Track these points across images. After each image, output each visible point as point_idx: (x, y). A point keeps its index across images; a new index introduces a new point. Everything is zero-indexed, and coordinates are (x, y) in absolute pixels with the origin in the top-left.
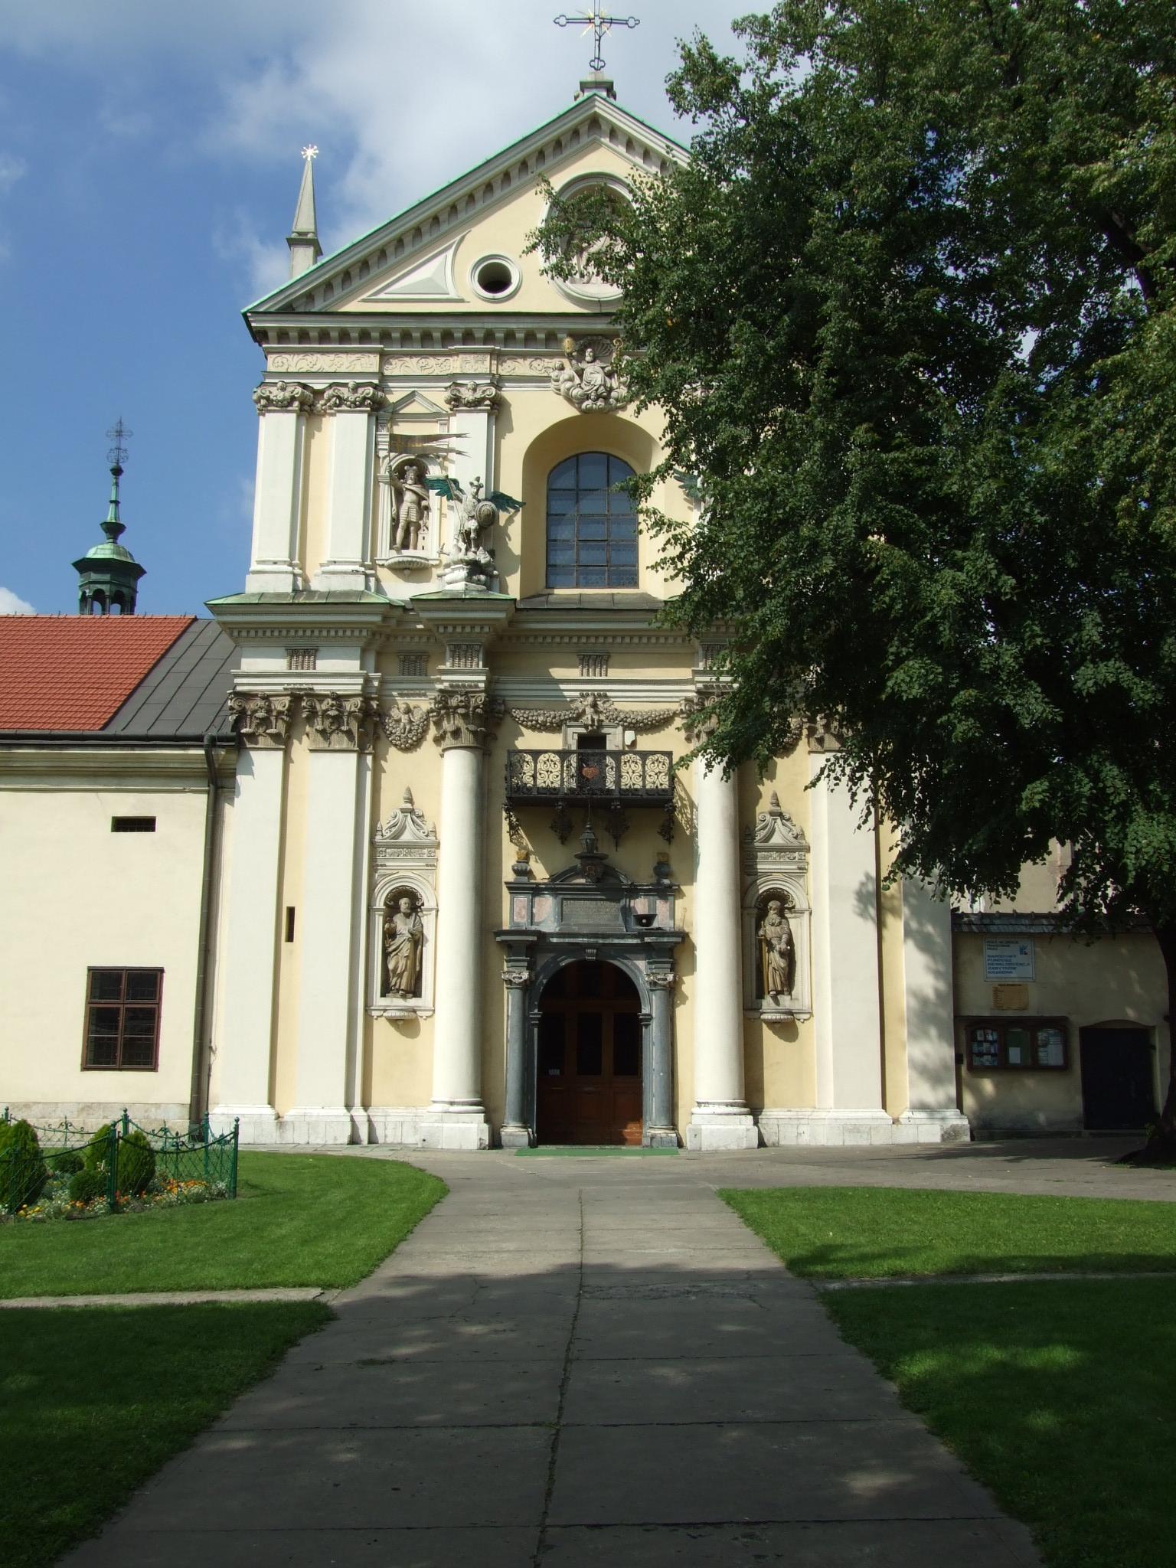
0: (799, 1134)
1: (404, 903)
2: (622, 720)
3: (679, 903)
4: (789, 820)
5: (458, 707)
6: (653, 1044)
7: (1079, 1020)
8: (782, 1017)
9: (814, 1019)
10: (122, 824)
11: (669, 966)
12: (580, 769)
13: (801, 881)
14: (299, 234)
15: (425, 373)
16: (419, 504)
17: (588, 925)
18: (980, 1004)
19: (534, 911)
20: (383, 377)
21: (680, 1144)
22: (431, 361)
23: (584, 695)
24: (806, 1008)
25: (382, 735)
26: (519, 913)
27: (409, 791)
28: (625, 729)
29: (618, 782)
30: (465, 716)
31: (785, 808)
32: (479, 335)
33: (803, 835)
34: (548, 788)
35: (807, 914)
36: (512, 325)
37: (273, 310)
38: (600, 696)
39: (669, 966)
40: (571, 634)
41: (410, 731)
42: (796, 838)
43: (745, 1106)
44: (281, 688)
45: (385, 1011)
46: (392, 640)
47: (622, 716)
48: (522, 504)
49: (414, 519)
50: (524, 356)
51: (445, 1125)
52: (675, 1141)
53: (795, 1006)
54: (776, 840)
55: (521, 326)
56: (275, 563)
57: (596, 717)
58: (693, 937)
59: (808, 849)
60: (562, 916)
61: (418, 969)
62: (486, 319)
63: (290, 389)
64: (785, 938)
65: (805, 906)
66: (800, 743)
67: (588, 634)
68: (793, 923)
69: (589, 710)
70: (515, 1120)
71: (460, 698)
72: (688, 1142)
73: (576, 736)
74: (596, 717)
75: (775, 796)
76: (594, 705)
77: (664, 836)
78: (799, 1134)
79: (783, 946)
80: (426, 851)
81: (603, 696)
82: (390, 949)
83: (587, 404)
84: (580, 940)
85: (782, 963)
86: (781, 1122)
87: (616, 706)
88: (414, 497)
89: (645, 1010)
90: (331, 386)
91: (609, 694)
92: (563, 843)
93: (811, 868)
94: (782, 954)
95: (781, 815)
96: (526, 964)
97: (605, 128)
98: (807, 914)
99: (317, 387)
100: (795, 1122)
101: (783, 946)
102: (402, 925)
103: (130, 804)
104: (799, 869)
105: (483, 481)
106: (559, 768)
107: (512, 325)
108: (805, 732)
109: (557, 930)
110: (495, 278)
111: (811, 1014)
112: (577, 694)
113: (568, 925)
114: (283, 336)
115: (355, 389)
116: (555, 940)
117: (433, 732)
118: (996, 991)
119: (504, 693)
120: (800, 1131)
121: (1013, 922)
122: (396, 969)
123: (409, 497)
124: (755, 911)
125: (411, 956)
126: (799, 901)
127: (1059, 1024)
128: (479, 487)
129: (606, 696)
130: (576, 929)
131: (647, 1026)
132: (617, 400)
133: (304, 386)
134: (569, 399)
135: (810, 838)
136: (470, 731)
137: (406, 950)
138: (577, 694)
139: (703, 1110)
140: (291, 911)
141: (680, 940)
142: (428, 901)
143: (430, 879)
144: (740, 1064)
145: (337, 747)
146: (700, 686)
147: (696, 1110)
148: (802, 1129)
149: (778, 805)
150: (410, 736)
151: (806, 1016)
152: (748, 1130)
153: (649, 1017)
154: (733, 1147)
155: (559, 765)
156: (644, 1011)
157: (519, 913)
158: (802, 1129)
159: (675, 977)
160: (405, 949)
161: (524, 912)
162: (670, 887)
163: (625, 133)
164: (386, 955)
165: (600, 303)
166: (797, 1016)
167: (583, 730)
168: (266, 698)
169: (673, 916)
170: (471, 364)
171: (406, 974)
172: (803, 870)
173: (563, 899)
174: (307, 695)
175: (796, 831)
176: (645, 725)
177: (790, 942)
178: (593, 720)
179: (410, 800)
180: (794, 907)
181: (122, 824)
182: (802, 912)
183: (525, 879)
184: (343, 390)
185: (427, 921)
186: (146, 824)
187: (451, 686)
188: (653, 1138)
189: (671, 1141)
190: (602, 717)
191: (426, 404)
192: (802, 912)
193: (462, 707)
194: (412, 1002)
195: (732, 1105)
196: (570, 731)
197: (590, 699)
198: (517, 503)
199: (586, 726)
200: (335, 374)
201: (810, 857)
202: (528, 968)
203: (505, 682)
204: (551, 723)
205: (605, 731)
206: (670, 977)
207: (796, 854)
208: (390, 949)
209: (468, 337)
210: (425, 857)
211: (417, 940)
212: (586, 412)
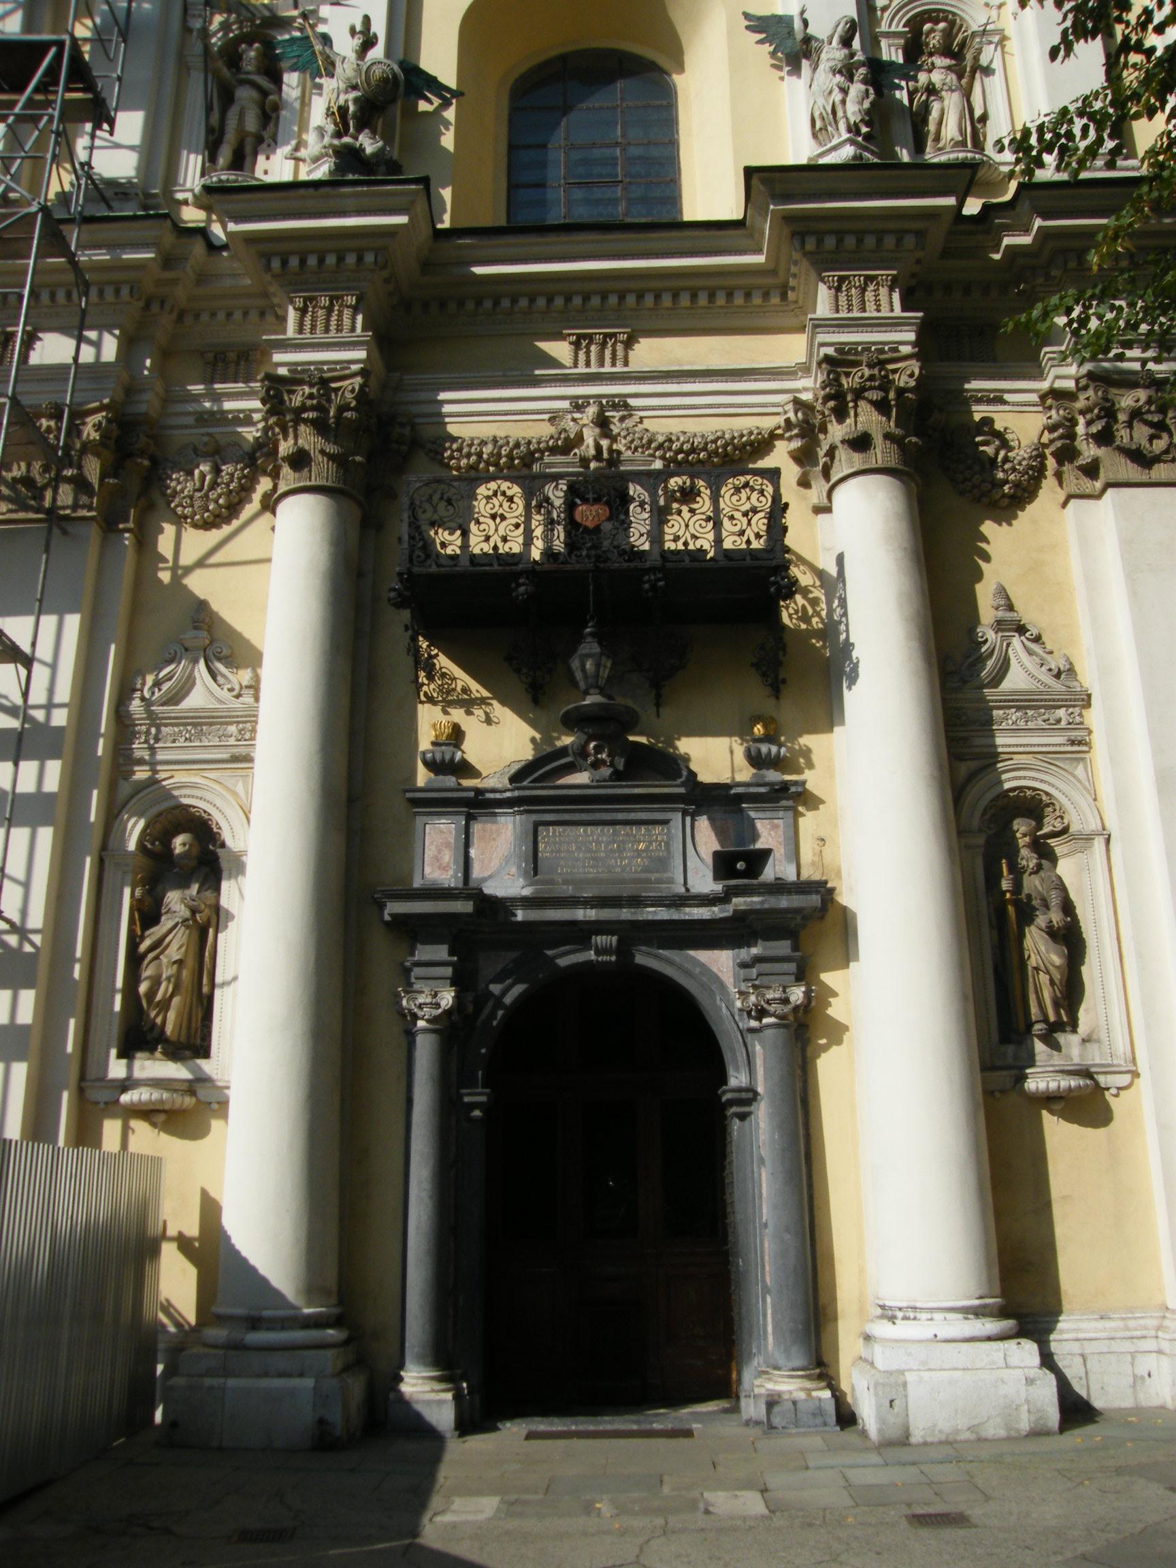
0: (1137, 1381)
2: (660, 446)
3: (809, 823)
4: (1037, 639)
5: (303, 408)
6: (762, 1161)
8: (1074, 1082)
9: (1143, 1083)
11: (792, 967)
12: (570, 507)
13: (1079, 771)
16: (262, 106)
17: (595, 881)
19: (473, 852)
21: (846, 1418)
23: (578, 405)
24: (1120, 1061)
25: (161, 503)
26: (437, 858)
29: (656, 536)
30: (320, 426)
31: (1027, 612)
33: (1071, 671)
34: (497, 556)
35: (1099, 843)
38: (615, 407)
39: (792, 967)
41: (214, 486)
42: (1058, 676)
43: (1002, 1313)
46: (189, 320)
47: (661, 439)
48: (457, 94)
51: (232, 1382)
52: (830, 1408)
53: (1095, 1057)
54: (1015, 680)
57: (605, 443)
58: (844, 898)
59: (1087, 701)
60: (534, 865)
61: (205, 989)
64: (1054, 899)
65: (1093, 825)
66: (1045, 483)
68: (1065, 868)
69: (590, 436)
70: (422, 1360)
71: (307, 390)
72: (867, 1411)
74: (605, 443)
75: (1002, 592)
76: (602, 423)
77: (764, 675)
78: (1137, 1380)
79: (1056, 917)
80: (233, 729)
81: (620, 403)
84: (580, 914)
85: (1056, 959)
86: (1090, 1348)
87: (647, 424)
88: (254, 94)
89: (737, 1079)
91: (631, 402)
92: (536, 701)
93: (1098, 740)
94: (1053, 933)
95: (1021, 629)
96: (448, 971)
98: (1099, 843)
100: (1127, 1346)
101: (1056, 917)
104: (1072, 743)
105: (379, 27)
106: (521, 510)
108: (1051, 463)
109: (527, 892)
111: (1135, 1074)
112: (565, 404)
113: (552, 882)
116: (520, 915)
119: (415, 409)
120: (1141, 1370)
123: (245, 95)
124: (980, 840)
125: (191, 963)
126: (1080, 817)
128: (368, 43)
129: (626, 406)
130: (569, 890)
131: (743, 1117)
135: (1088, 677)
136: (331, 457)
138: (565, 404)
139: (902, 1330)
141: (815, 900)
143: (240, 788)
144: (983, 1212)
146: (830, 351)
147: (882, 1329)
148: (1147, 1363)
149: (1010, 607)
150: (213, 495)
151: (1124, 1080)
152: (1030, 1381)
153: (749, 1097)
154: (994, 1430)
155: (519, 501)
156: (733, 1082)
157: (437, 858)
158: (1147, 1363)
159: (807, 994)
160: (174, 946)
161: (447, 856)
162: (784, 787)
164: (135, 960)
166: (1102, 1079)
169: (795, 855)
171: (176, 1001)
172: (1080, 743)
173: (537, 825)
175: (1056, 662)
177: (1068, 907)
178: (598, 448)
180: (1065, 831)
182: (1088, 838)
183: (450, 781)
188: (772, 1402)
189: (819, 1412)
190: (620, 446)
192: (1088, 838)
193: (313, 408)
195: (978, 1312)
197: (592, 411)
198: (448, 89)
199: (584, 461)
201: (1094, 717)
202: (455, 981)
203: (418, 403)
204: (511, 457)
206: (797, 994)
207: (1061, 713)
208: (143, 947)
210: (232, 741)
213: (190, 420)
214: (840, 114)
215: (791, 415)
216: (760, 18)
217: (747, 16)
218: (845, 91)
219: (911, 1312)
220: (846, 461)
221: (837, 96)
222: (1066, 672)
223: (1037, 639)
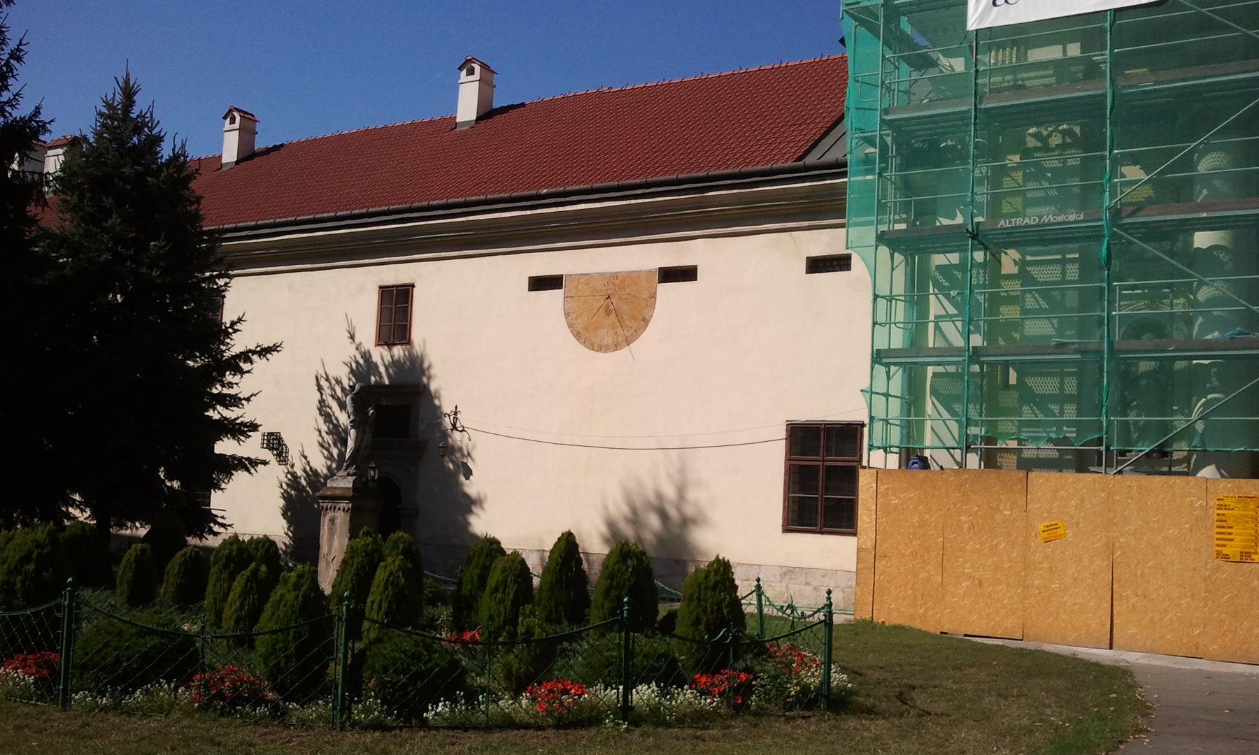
10: (817, 265)
181: (817, 265)
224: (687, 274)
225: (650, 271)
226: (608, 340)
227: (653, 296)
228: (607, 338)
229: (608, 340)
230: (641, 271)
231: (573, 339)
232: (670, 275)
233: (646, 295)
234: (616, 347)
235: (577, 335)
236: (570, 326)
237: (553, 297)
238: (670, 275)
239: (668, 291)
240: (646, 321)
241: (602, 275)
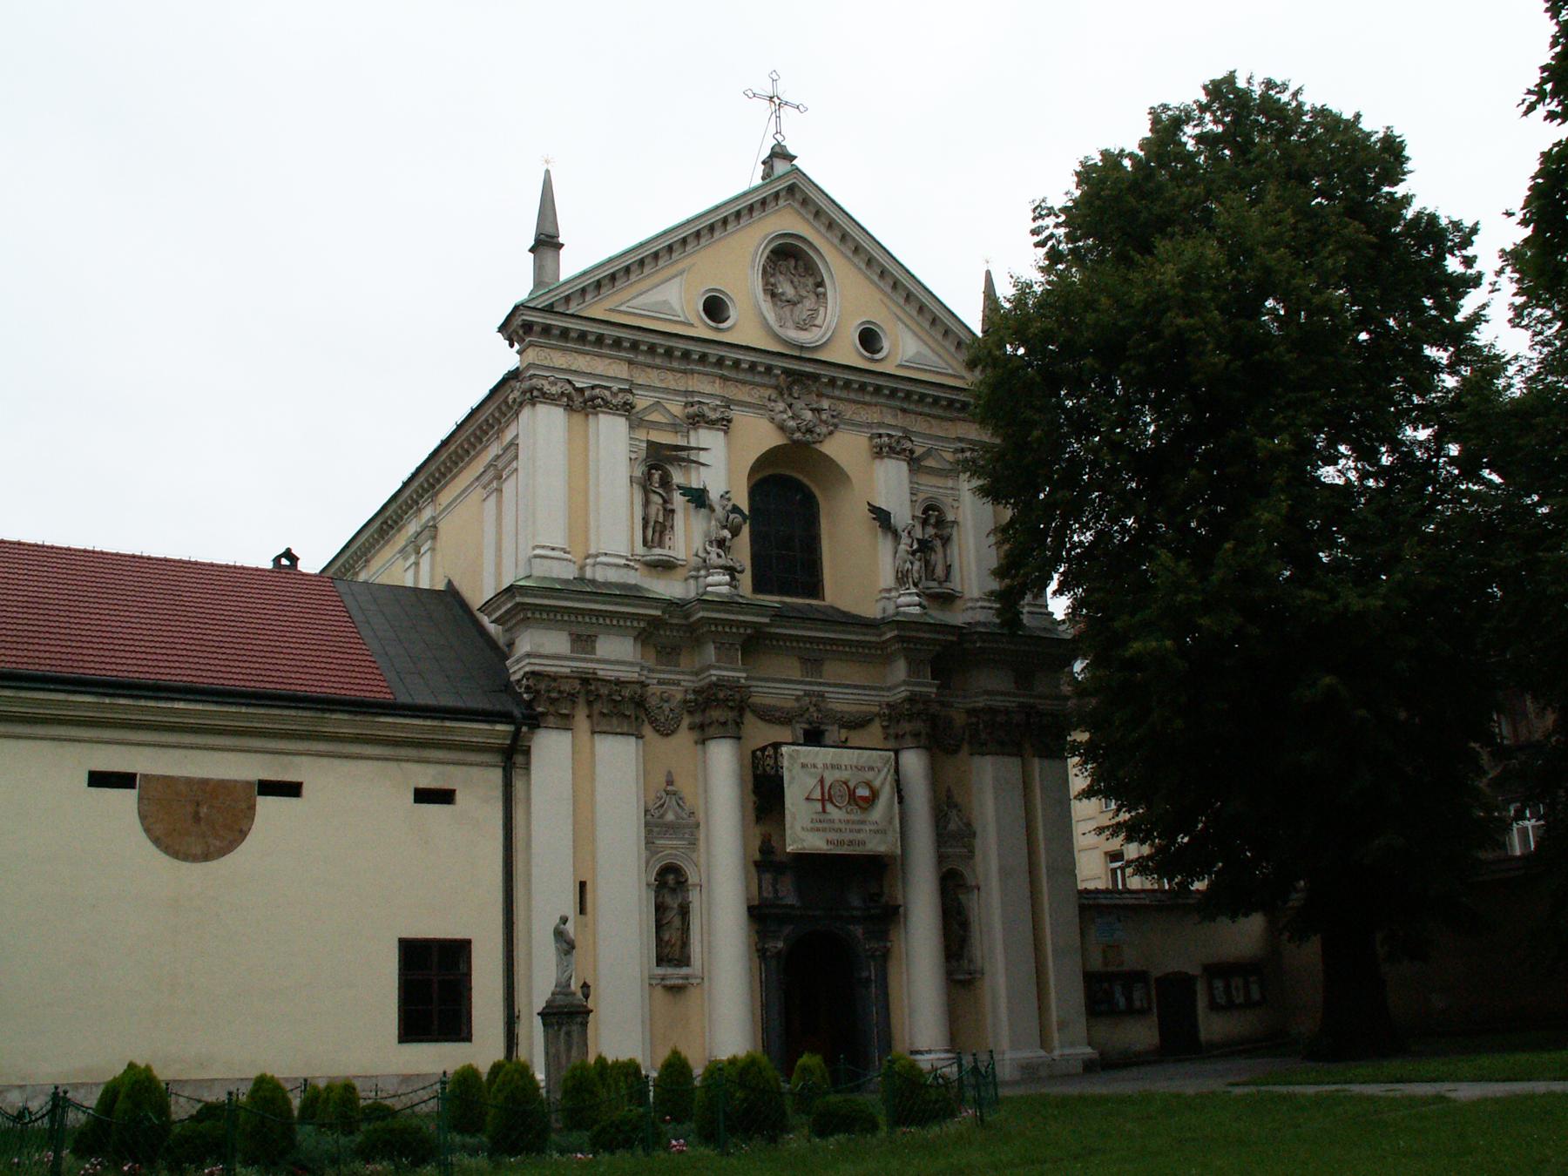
1: (671, 878)
7: (1156, 973)
14: (548, 236)
15: (664, 386)
18: (1096, 964)
20: (632, 383)
22: (670, 376)
23: (807, 693)
27: (669, 773)
28: (842, 726)
32: (713, 360)
36: (691, 346)
37: (539, 307)
40: (798, 639)
44: (568, 670)
45: (663, 979)
49: (661, 520)
50: (744, 383)
55: (763, 361)
56: (553, 549)
62: (674, 339)
63: (560, 384)
67: (811, 640)
73: (802, 731)
80: (687, 830)
81: (821, 695)
82: (665, 922)
83: (797, 435)
87: (831, 706)
88: (661, 501)
90: (593, 387)
91: (826, 695)
97: (798, 196)
98: (976, 891)
99: (578, 385)
102: (673, 902)
103: (429, 777)
107: (723, 352)
110: (715, 308)
114: (546, 330)
115: (615, 395)
117: (686, 721)
118: (1104, 951)
121: (1109, 896)
122: (670, 940)
123: (656, 499)
127: (1140, 976)
132: (819, 434)
133: (569, 382)
134: (782, 428)
135: (977, 827)
137: (677, 922)
138: (801, 693)
140: (583, 885)
142: (692, 878)
145: (618, 730)
146: (908, 693)
163: (815, 204)
165: (802, 348)
167: (806, 726)
168: (554, 678)
170: (706, 386)
174: (594, 679)
176: (856, 724)
179: (670, 782)
184: (607, 393)
185: (694, 897)
186: (444, 796)
187: (719, 679)
191: (667, 416)
194: (684, 971)
195: (947, 1051)
196: (798, 726)
200: (601, 377)
201: (978, 842)
205: (823, 727)
208: (665, 922)
209: (703, 358)
210: (686, 836)
211: (684, 911)
212: (796, 442)
213: (655, 681)
214: (910, 575)
215: (886, 711)
216: (874, 507)
217: (869, 503)
218: (912, 563)
219: (929, 1052)
220: (909, 741)
221: (908, 565)
222: (969, 825)
223: (960, 811)
224: (292, 790)
225: (249, 784)
226: (198, 850)
227: (252, 808)
228: (198, 850)
229: (198, 850)
230: (236, 781)
231: (149, 844)
232: (270, 788)
233: (244, 806)
234: (206, 857)
235: (157, 841)
236: (147, 830)
237: (126, 799)
238: (270, 788)
239: (267, 806)
240: (243, 834)
241: (189, 781)
